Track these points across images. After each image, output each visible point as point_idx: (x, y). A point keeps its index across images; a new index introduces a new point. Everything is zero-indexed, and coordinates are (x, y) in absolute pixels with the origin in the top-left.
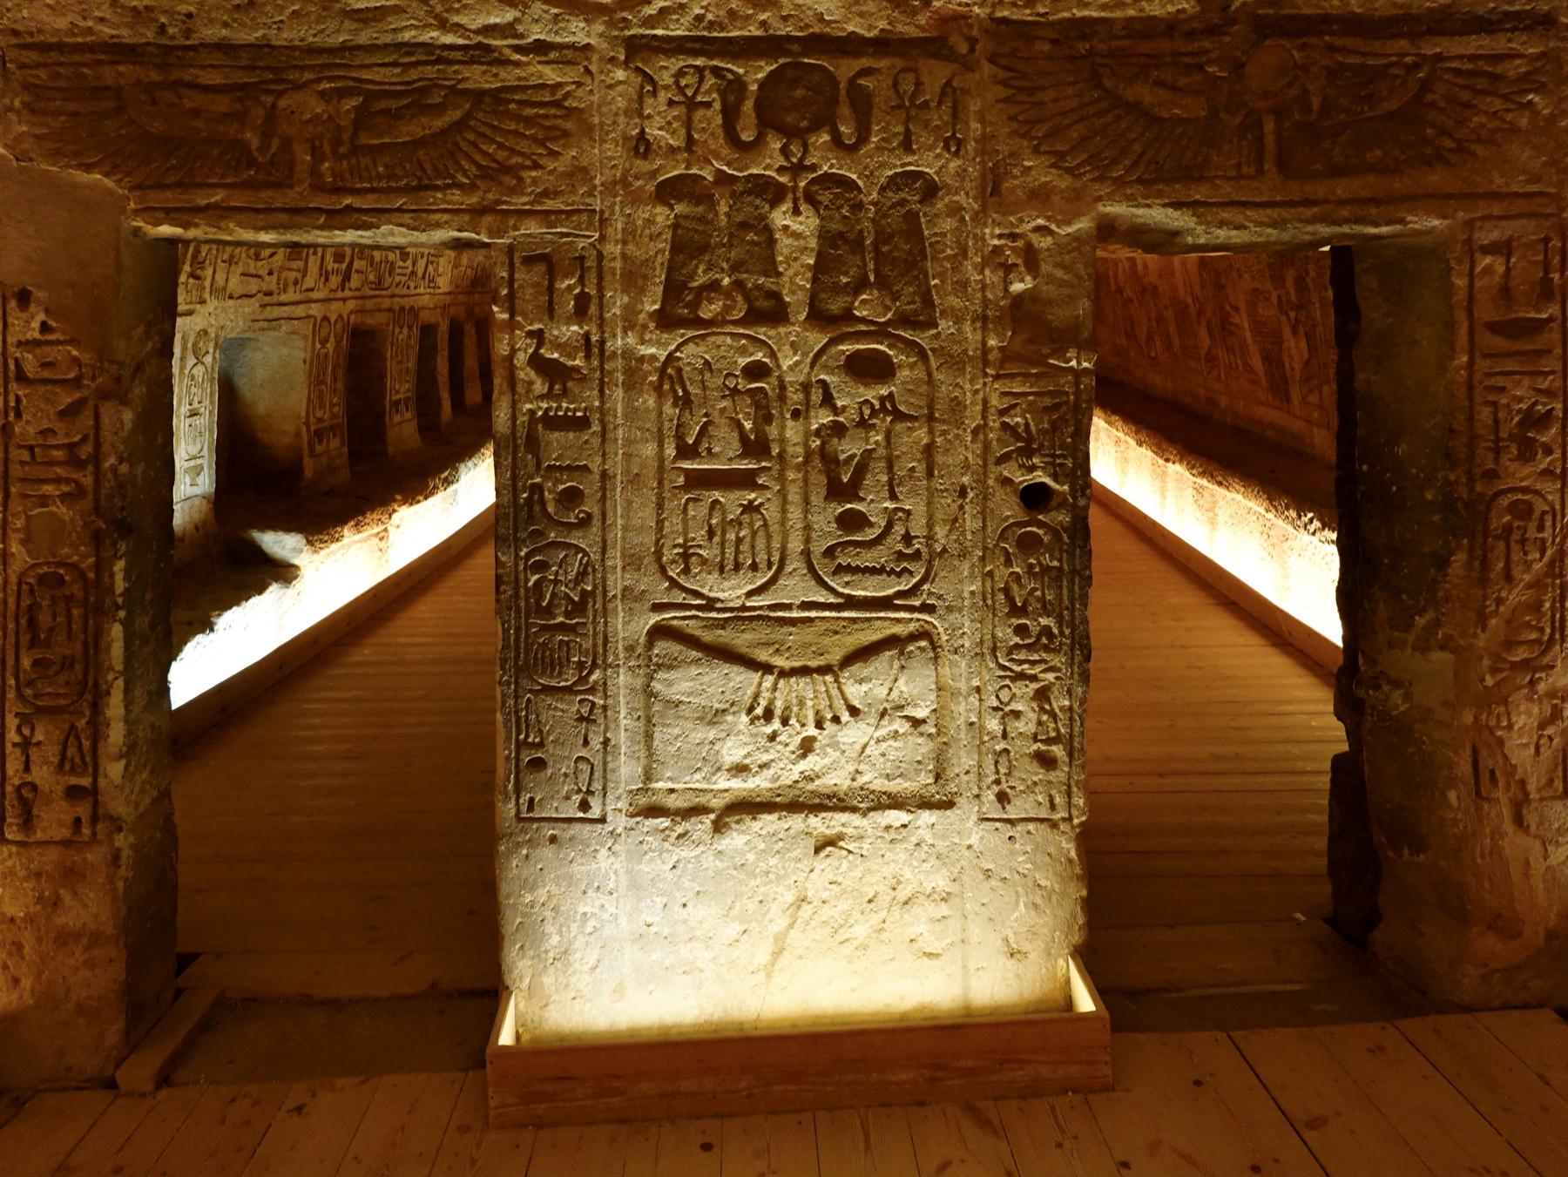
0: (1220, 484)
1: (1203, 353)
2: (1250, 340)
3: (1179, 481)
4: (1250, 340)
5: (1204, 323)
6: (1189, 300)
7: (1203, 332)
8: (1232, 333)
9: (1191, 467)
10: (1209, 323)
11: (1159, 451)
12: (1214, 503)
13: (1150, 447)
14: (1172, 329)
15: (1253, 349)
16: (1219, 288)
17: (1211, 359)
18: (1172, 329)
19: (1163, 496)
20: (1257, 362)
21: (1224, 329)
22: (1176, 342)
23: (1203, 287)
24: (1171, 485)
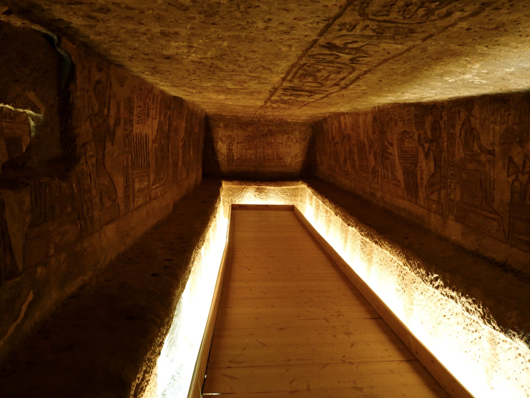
0: (376, 243)
1: (371, 169)
2: (397, 162)
3: (354, 235)
4: (397, 162)
5: (372, 153)
6: (366, 141)
7: (371, 157)
8: (387, 158)
9: (361, 231)
10: (375, 152)
11: (346, 219)
12: (372, 251)
13: (341, 216)
14: (356, 157)
15: (398, 166)
16: (383, 132)
17: (374, 172)
18: (356, 157)
19: (346, 242)
20: (400, 175)
21: (384, 155)
22: (357, 163)
23: (374, 133)
24: (350, 236)
